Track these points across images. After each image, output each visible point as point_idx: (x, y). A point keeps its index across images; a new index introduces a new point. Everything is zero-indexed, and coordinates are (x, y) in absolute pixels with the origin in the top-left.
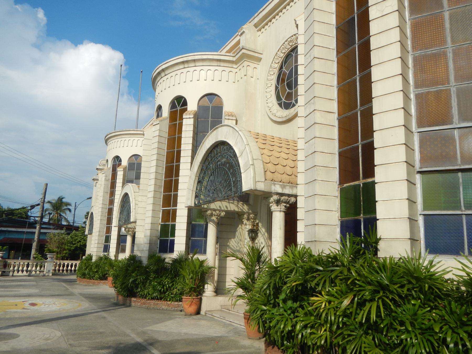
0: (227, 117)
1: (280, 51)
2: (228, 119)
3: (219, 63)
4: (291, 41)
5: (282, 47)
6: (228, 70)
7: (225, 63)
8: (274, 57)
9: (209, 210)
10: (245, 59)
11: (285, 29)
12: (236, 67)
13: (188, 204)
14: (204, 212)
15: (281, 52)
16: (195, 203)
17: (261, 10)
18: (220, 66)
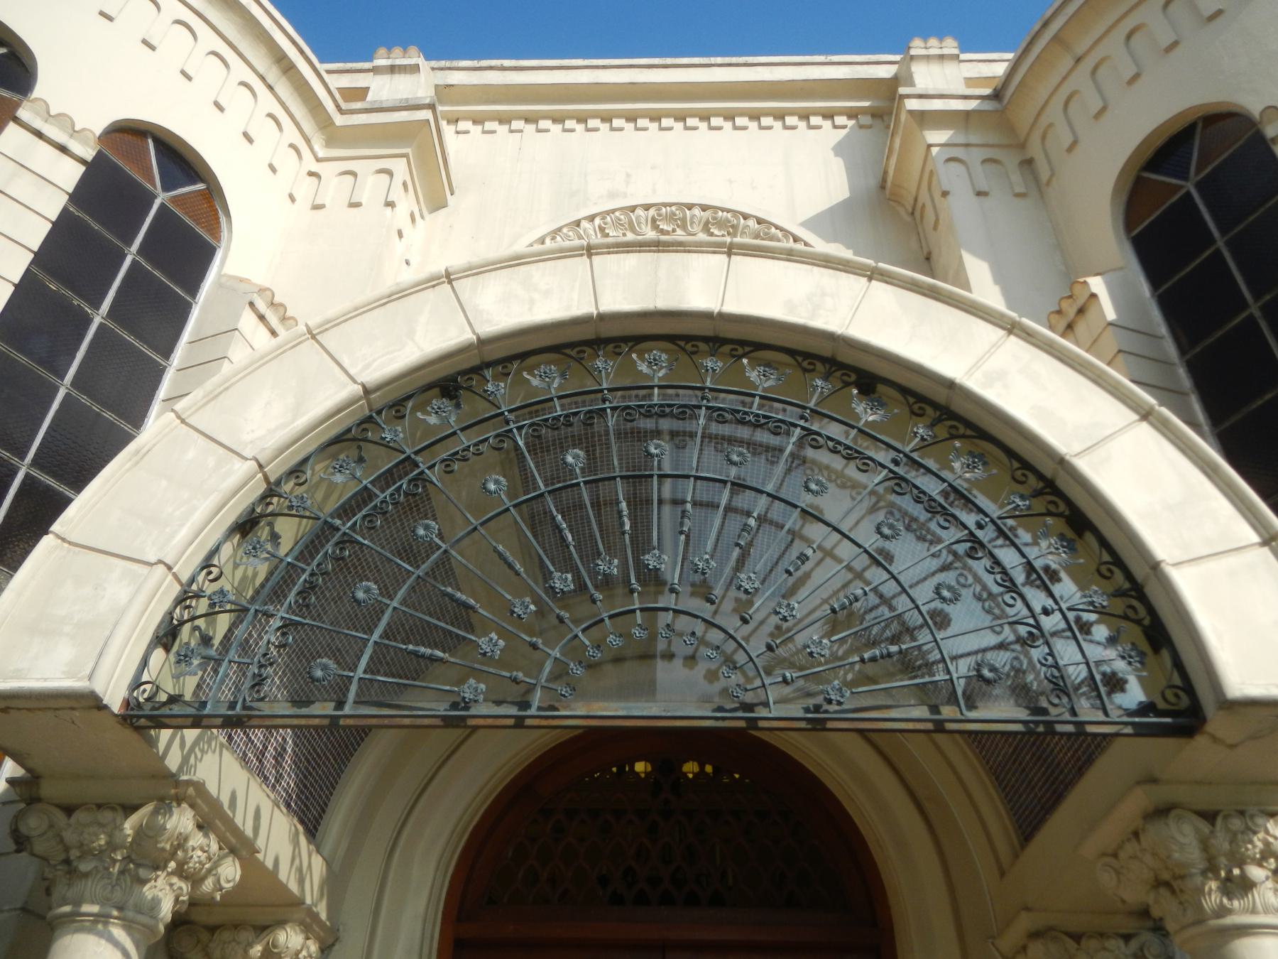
0: (262, 306)
1: (597, 221)
2: (262, 318)
3: (273, 75)
4: (671, 218)
5: (617, 214)
6: (292, 135)
7: (299, 99)
8: (560, 229)
9: (179, 800)
10: (408, 150)
11: (628, 175)
12: (321, 154)
13: (18, 674)
14: (69, 810)
15: (602, 229)
16: (137, 684)
17: (507, 63)
18: (270, 88)
